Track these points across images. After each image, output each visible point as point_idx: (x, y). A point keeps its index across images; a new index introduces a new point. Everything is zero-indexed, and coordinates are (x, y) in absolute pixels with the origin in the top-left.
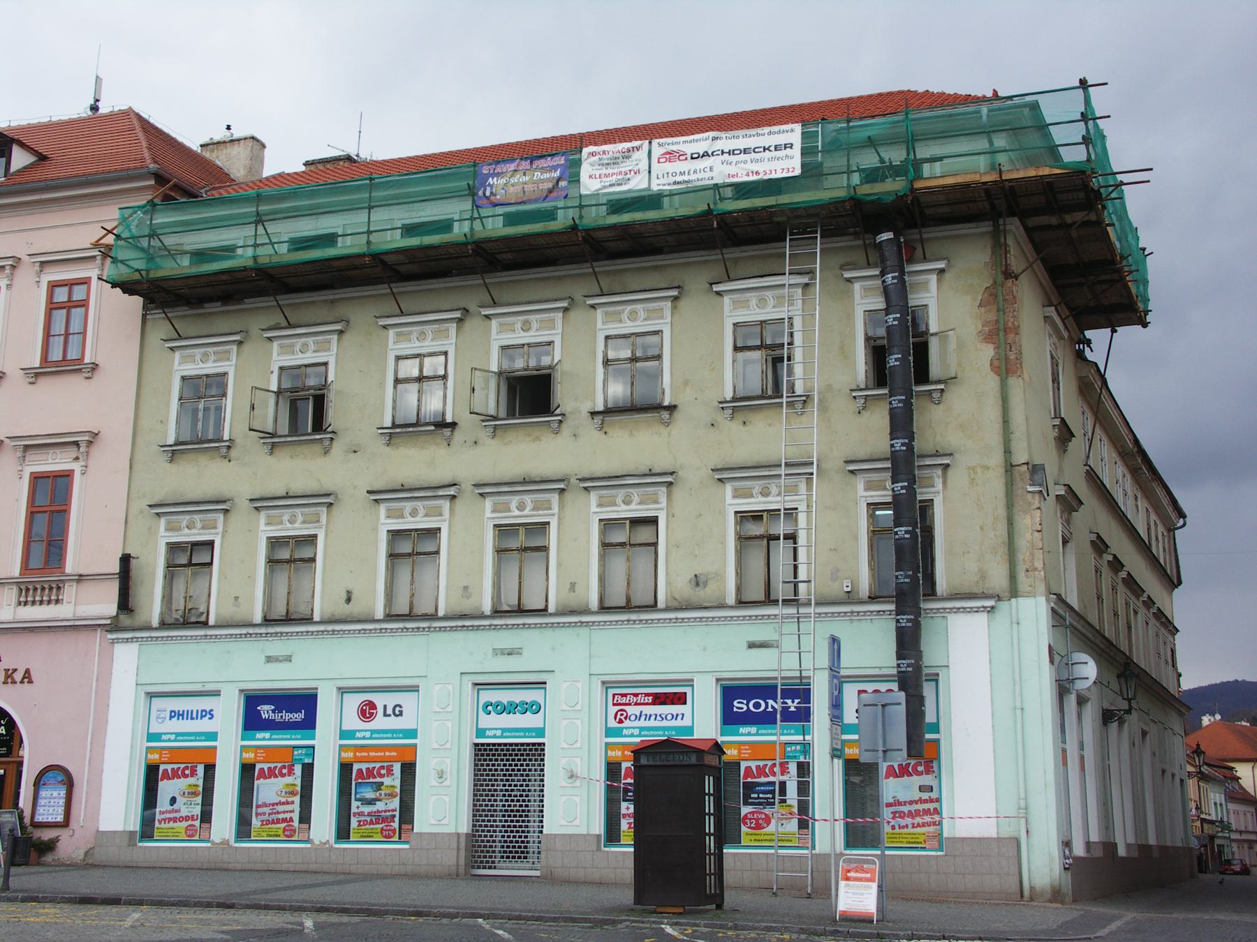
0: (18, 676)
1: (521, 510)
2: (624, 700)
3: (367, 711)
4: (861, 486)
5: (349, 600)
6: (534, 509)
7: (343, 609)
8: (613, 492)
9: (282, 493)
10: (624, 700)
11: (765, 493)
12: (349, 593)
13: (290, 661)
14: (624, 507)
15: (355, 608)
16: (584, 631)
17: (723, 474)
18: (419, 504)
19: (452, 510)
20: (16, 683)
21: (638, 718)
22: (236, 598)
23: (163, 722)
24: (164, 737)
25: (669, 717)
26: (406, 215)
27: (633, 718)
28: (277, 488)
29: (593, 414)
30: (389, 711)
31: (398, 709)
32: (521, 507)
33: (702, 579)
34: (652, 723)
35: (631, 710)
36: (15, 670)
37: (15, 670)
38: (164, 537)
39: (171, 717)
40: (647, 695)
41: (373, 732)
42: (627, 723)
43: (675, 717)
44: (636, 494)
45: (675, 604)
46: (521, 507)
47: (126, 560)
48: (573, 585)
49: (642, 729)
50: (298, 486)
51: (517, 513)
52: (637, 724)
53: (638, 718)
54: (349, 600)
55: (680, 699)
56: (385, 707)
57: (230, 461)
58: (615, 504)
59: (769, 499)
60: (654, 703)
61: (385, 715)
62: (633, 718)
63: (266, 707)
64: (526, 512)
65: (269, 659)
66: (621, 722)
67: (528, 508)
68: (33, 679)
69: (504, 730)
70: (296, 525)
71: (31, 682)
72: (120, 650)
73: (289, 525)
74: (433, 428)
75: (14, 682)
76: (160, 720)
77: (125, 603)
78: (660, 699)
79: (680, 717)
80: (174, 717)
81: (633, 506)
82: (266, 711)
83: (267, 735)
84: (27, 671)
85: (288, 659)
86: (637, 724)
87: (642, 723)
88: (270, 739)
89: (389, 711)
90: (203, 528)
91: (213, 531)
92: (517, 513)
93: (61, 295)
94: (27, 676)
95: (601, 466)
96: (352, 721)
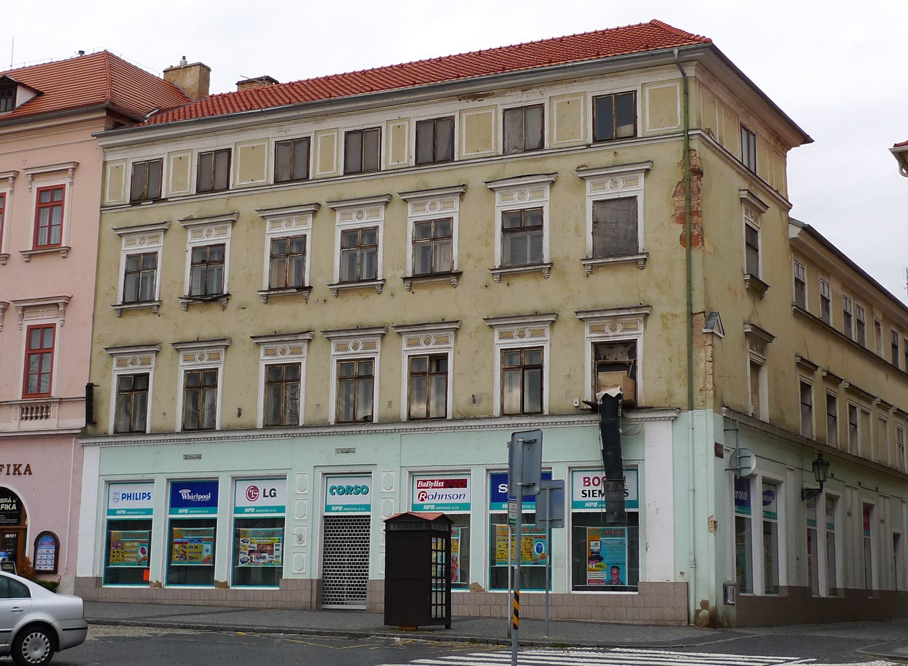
0: (22, 470)
1: (355, 351)
2: (425, 485)
3: (252, 494)
4: (587, 330)
5: (239, 415)
6: (365, 348)
7: (236, 421)
8: (418, 335)
9: (194, 338)
10: (425, 485)
11: (521, 336)
12: (239, 410)
13: (200, 458)
14: (425, 346)
15: (244, 420)
16: (397, 436)
17: (493, 322)
18: (287, 346)
19: (308, 349)
20: (21, 474)
21: (434, 497)
22: (165, 414)
23: (117, 501)
24: (118, 512)
25: (455, 497)
26: (278, 134)
27: (431, 497)
28: (191, 335)
29: (405, 279)
30: (267, 493)
31: (273, 492)
32: (355, 347)
33: (477, 398)
34: (443, 501)
35: (430, 492)
36: (20, 465)
37: (20, 465)
38: (116, 371)
39: (123, 498)
40: (440, 481)
41: (256, 508)
42: (426, 501)
43: (459, 497)
44: (433, 337)
45: (459, 416)
46: (355, 347)
47: (90, 387)
48: (390, 403)
49: (436, 505)
50: (206, 333)
51: (353, 351)
52: (433, 501)
53: (434, 497)
54: (239, 415)
55: (462, 484)
56: (265, 490)
57: (159, 316)
58: (419, 344)
59: (525, 340)
60: (445, 487)
61: (265, 496)
62: (431, 497)
63: (185, 491)
64: (358, 351)
65: (187, 457)
66: (422, 500)
67: (360, 348)
68: (32, 472)
69: (344, 506)
70: (204, 362)
71: (30, 473)
72: (87, 450)
73: (199, 362)
74: (296, 291)
75: (19, 474)
76: (115, 500)
77: (91, 419)
78: (449, 484)
79: (462, 497)
80: (125, 498)
81: (431, 346)
82: (185, 494)
83: (186, 510)
84: (28, 466)
85: (199, 457)
86: (433, 501)
87: (437, 501)
88: (188, 514)
89: (267, 493)
90: (142, 364)
91: (148, 366)
92: (353, 351)
93: (47, 199)
94: (28, 469)
95: (411, 316)
96: (243, 501)
